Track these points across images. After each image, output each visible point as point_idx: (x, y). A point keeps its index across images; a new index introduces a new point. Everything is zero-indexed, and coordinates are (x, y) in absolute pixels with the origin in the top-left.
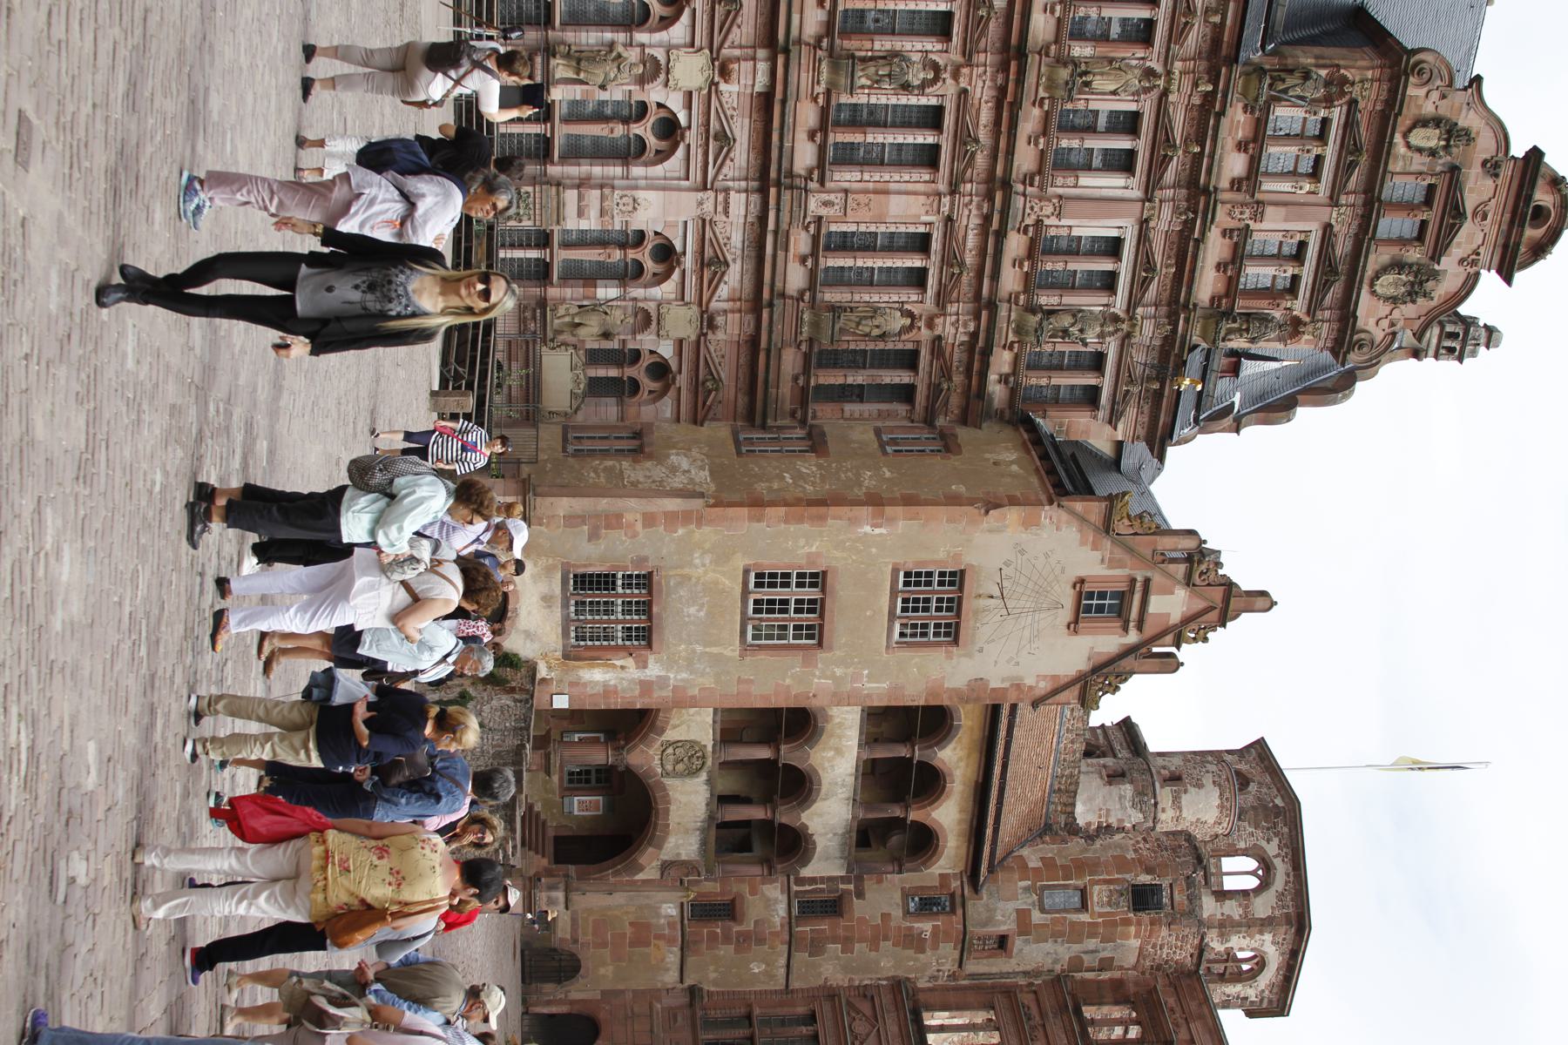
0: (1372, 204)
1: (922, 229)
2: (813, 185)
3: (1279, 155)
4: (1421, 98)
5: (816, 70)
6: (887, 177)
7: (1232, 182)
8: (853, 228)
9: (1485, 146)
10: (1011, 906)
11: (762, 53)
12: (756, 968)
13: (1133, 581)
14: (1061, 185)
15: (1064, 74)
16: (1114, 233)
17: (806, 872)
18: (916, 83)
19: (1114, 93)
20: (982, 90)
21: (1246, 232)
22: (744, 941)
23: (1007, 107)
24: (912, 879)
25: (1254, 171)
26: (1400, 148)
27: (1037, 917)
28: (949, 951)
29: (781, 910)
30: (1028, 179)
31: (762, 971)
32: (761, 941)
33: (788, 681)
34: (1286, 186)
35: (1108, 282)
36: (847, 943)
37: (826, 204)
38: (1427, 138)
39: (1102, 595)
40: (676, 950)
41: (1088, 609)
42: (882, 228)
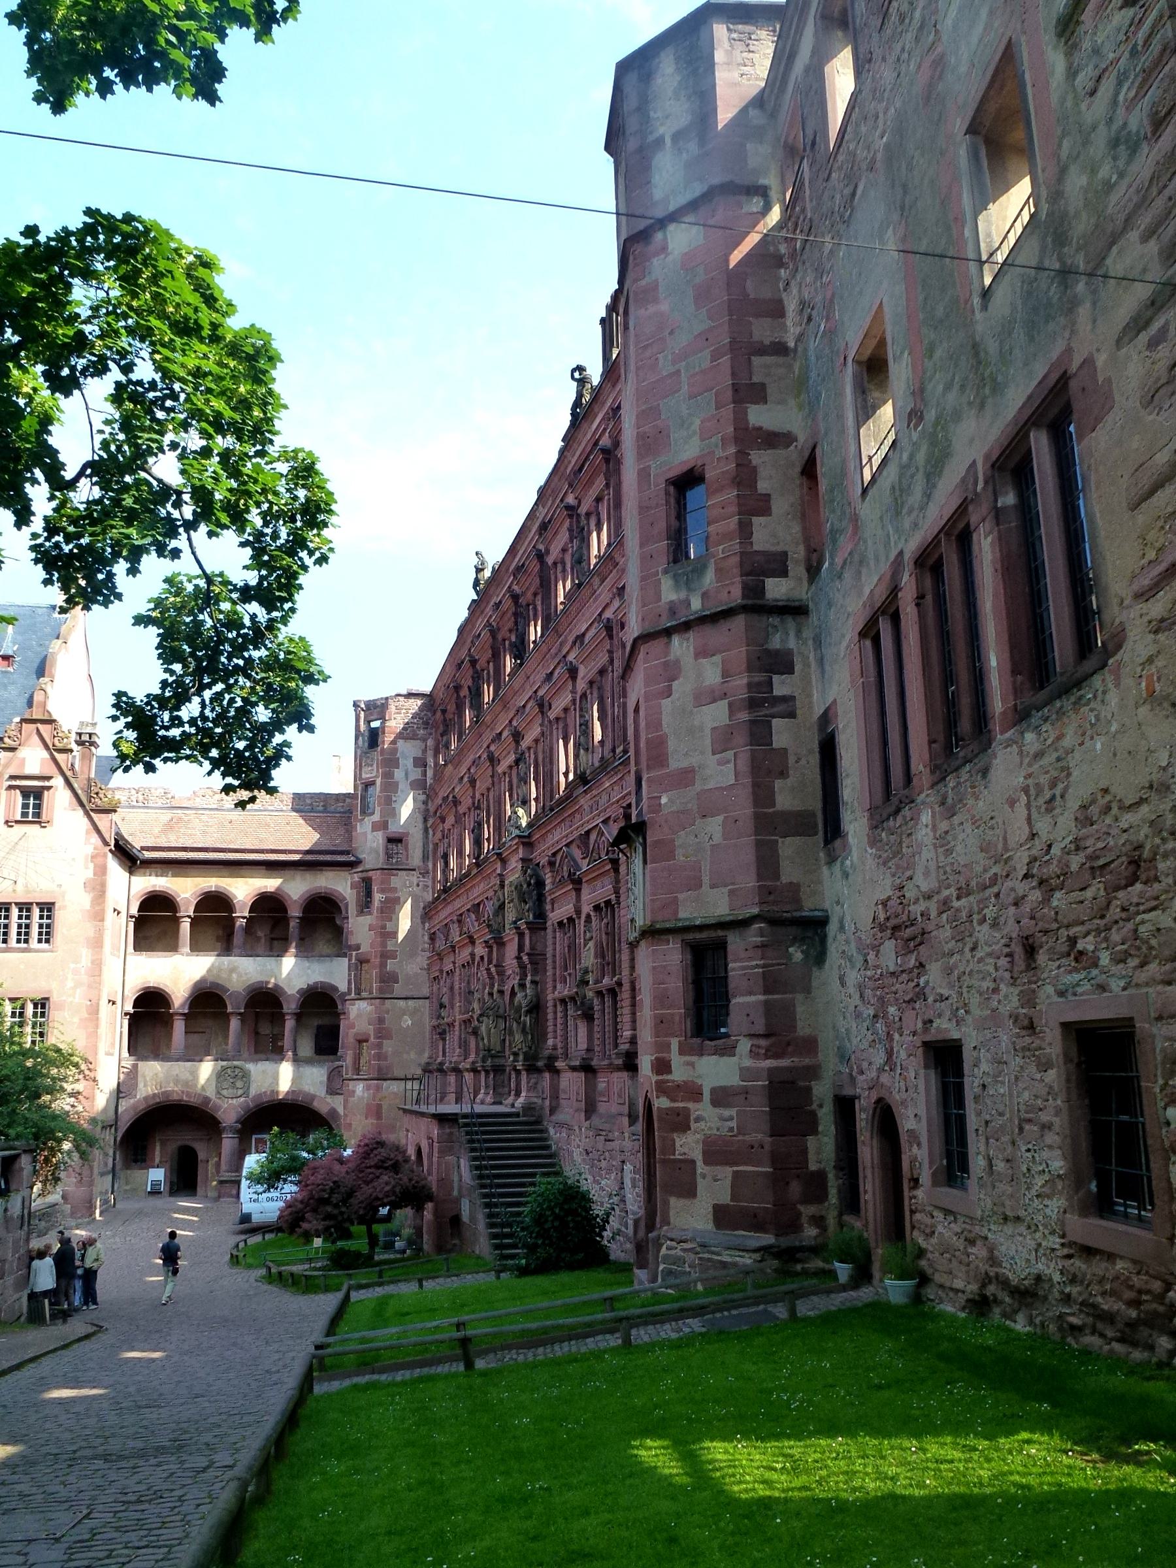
10: (369, 837)
12: (408, 1022)
13: (10, 787)
17: (343, 987)
22: (383, 1033)
24: (352, 910)
27: (376, 817)
28: (397, 881)
29: (363, 1005)
31: (411, 1018)
32: (381, 1020)
33: (76, 1020)
36: (385, 956)
39: (25, 806)
40: (385, 1084)
41: (38, 815)
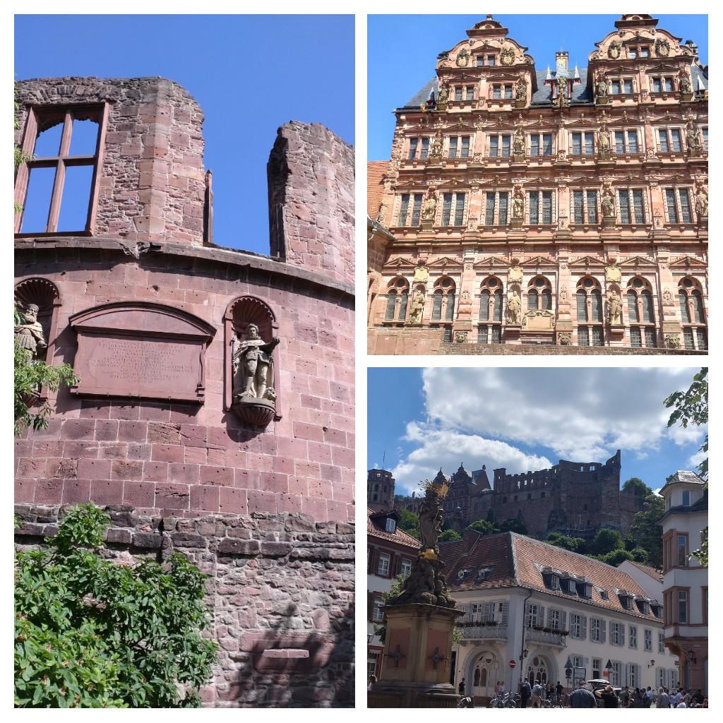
0: (638, 61)
1: (664, 191)
2: (652, 229)
3: (624, 89)
4: (604, 56)
5: (610, 230)
6: (646, 204)
7: (635, 101)
8: (667, 214)
9: (616, 38)
11: (605, 248)
14: (643, 149)
15: (603, 153)
16: (658, 132)
18: (610, 198)
19: (609, 139)
20: (612, 178)
21: (651, 94)
23: (615, 169)
25: (632, 95)
26: (619, 58)
30: (641, 160)
34: (635, 86)
35: (676, 132)
37: (658, 223)
38: (614, 53)
42: (666, 204)
